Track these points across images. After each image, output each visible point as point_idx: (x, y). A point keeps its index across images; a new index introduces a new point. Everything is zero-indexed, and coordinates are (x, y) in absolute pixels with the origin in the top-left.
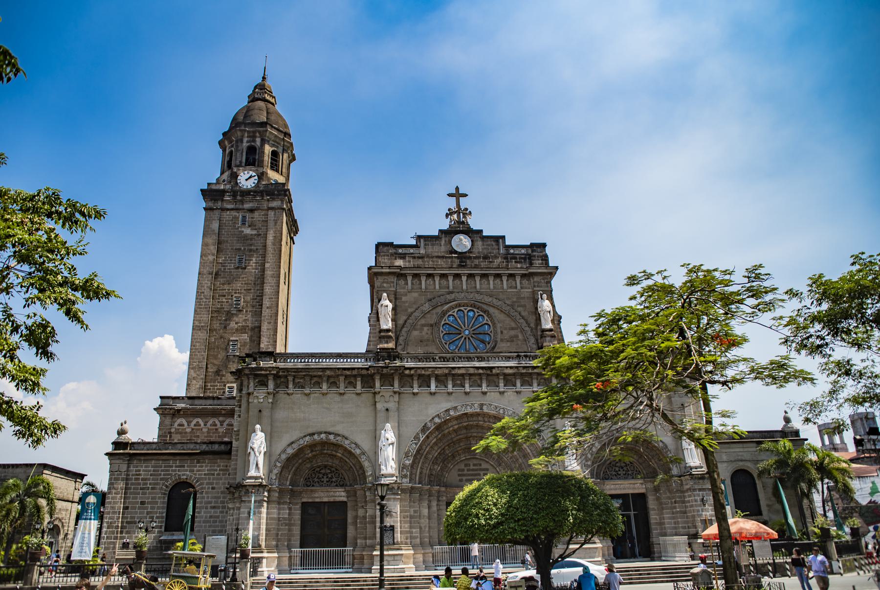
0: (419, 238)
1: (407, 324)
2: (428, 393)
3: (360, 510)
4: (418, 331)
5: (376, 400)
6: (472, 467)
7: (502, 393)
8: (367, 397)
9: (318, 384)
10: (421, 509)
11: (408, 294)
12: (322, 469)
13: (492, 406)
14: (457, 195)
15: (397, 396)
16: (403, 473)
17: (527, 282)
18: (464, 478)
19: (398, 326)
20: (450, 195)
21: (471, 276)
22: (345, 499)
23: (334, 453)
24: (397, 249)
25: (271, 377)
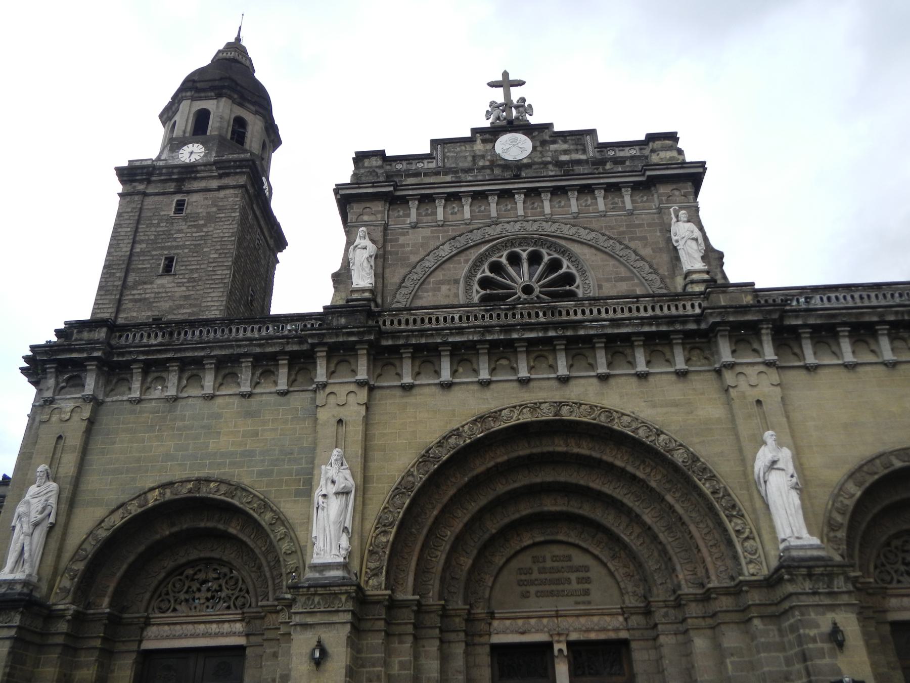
0: (435, 143)
1: (407, 283)
2: (435, 384)
3: (269, 663)
4: (430, 294)
5: (318, 403)
6: (549, 564)
7: (604, 378)
8: (299, 400)
9: (196, 378)
10: (423, 661)
11: (410, 231)
12: (200, 570)
13: (583, 406)
14: (506, 83)
15: (363, 395)
16: (372, 565)
17: (645, 198)
18: (533, 589)
19: (391, 288)
20: (493, 85)
21: (532, 194)
22: (242, 641)
23: (221, 526)
24: (394, 164)
25: (92, 366)
